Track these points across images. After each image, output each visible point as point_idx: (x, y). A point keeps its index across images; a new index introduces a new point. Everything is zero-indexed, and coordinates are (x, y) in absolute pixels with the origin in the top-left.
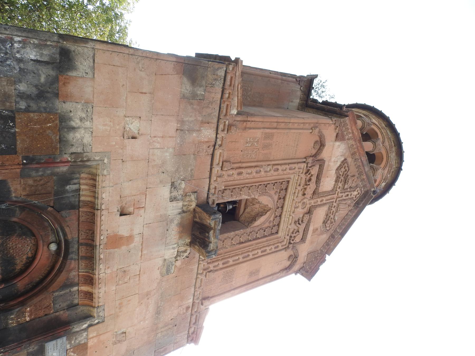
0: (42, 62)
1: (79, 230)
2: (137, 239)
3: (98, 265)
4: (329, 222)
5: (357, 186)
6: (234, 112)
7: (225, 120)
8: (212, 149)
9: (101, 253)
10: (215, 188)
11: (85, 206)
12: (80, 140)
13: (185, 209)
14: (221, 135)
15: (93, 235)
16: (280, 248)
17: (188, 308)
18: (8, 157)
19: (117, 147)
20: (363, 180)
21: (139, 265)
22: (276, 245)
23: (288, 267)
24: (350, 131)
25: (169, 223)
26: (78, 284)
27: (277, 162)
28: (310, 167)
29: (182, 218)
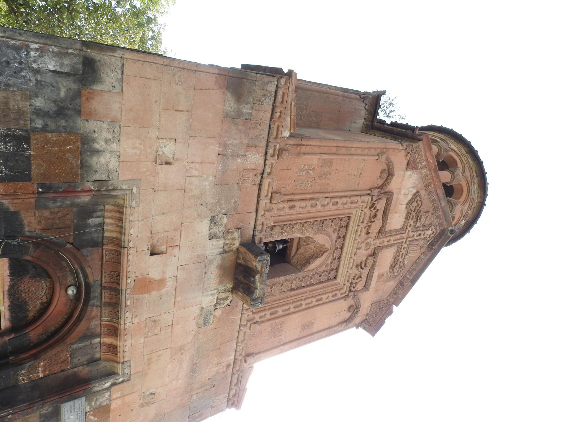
0: (62, 73)
1: (102, 271)
2: (170, 283)
3: (123, 313)
4: (397, 266)
5: (431, 224)
6: (286, 134)
7: (275, 144)
8: (260, 178)
9: (128, 299)
10: (263, 224)
11: (110, 243)
12: (105, 166)
13: (226, 248)
14: (270, 161)
15: (118, 278)
16: (339, 296)
17: (228, 366)
18: (21, 184)
19: (148, 173)
20: (438, 217)
21: (172, 313)
22: (334, 293)
23: (348, 319)
24: (424, 158)
26: (100, 336)
27: (336, 194)
28: (375, 201)
29: (223, 259)
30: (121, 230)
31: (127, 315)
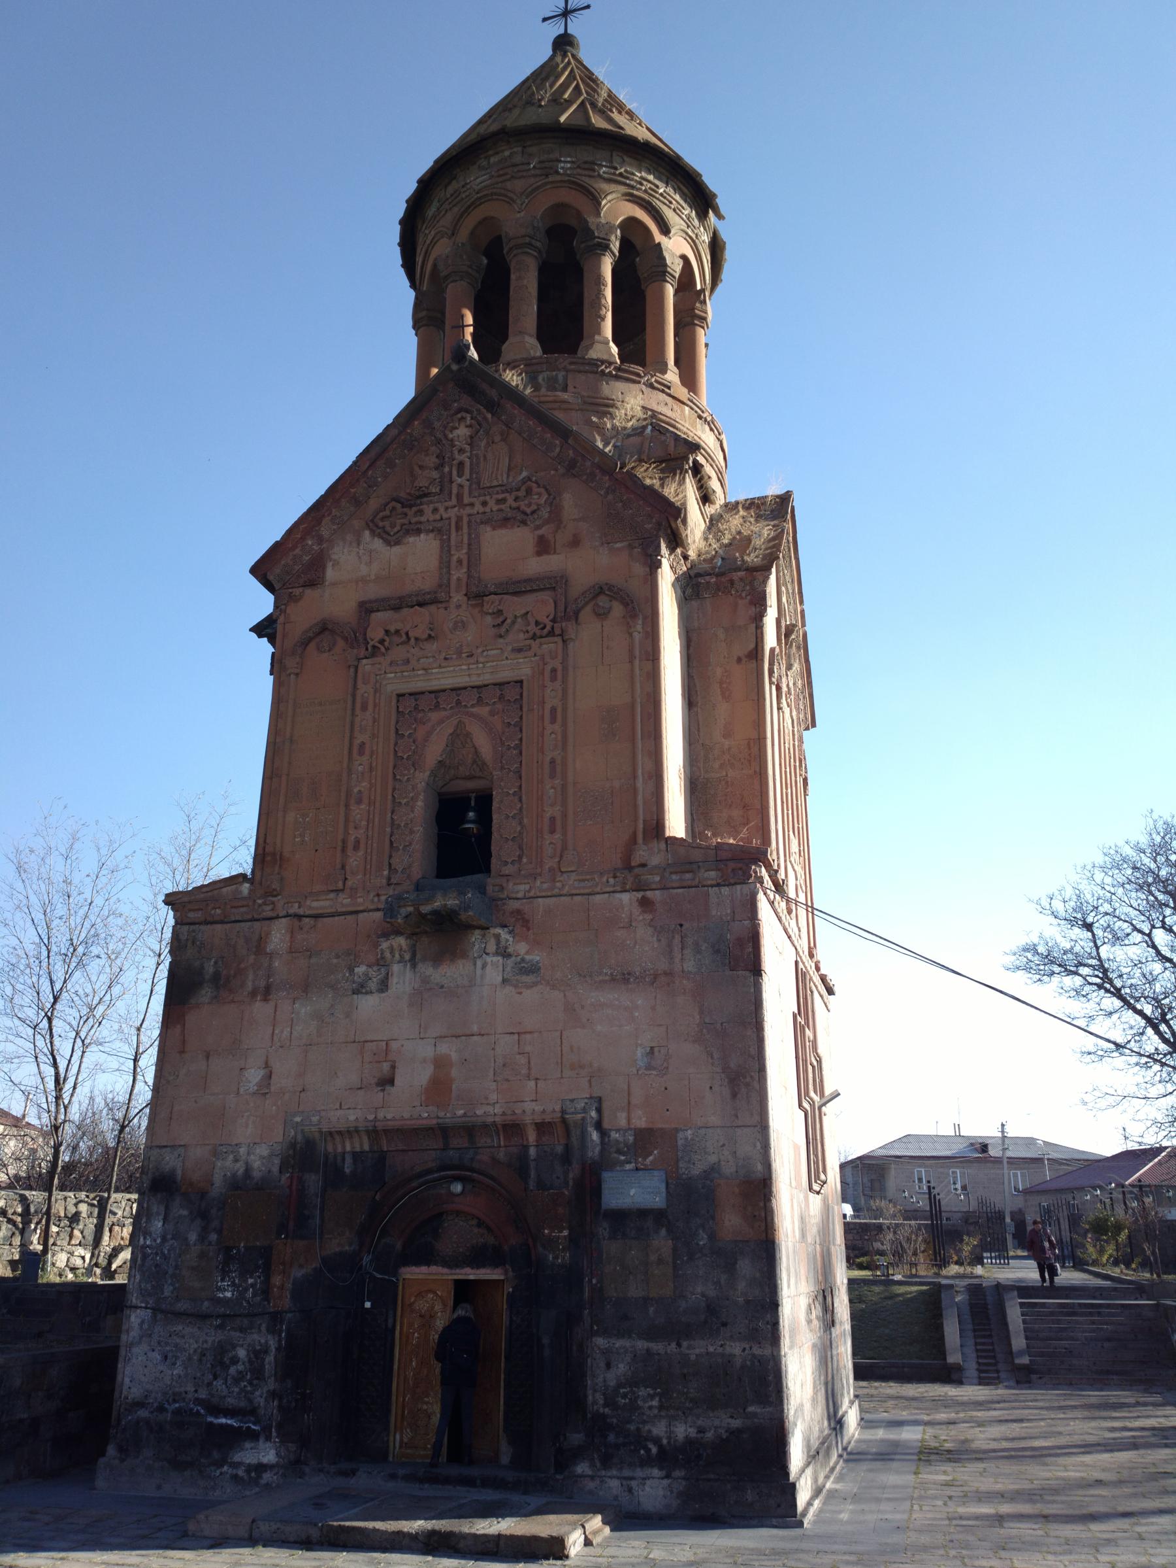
2: (444, 1048)
4: (522, 505)
8: (307, 920)
13: (407, 957)
16: (557, 664)
17: (645, 903)
24: (297, 551)
26: (526, 1148)
27: (346, 752)
30: (350, 1133)
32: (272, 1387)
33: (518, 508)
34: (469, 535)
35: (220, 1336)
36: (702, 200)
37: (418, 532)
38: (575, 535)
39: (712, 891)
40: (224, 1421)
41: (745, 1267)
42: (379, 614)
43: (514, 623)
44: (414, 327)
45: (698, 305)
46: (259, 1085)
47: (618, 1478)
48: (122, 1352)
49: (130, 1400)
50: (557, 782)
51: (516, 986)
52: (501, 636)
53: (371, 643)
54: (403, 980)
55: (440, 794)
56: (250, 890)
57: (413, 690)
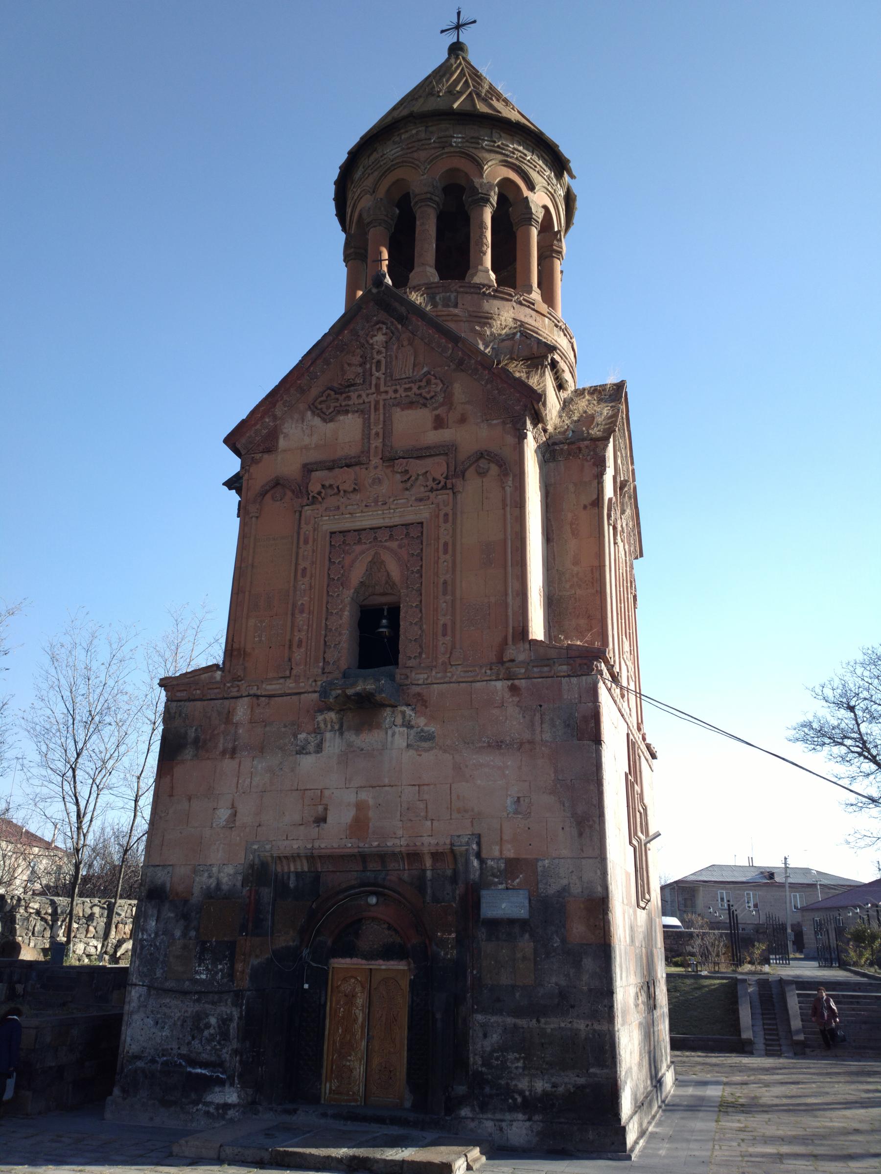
2: (363, 795)
4: (424, 392)
13: (337, 727)
16: (448, 509)
17: (514, 689)
24: (258, 427)
25: (352, 749)
26: (424, 871)
27: (292, 575)
30: (294, 857)
31: (389, 844)
32: (235, 1047)
33: (420, 394)
34: (384, 414)
35: (198, 1007)
36: (559, 164)
37: (347, 412)
38: (462, 415)
39: (564, 680)
40: (199, 1071)
41: (589, 964)
42: (317, 473)
43: (417, 479)
44: (344, 261)
45: (555, 242)
46: (227, 821)
47: (492, 1120)
48: (125, 1018)
49: (130, 1054)
50: (448, 597)
51: (417, 750)
52: (407, 489)
53: (312, 494)
54: (333, 744)
55: (361, 606)
56: (222, 676)
57: (343, 529)
